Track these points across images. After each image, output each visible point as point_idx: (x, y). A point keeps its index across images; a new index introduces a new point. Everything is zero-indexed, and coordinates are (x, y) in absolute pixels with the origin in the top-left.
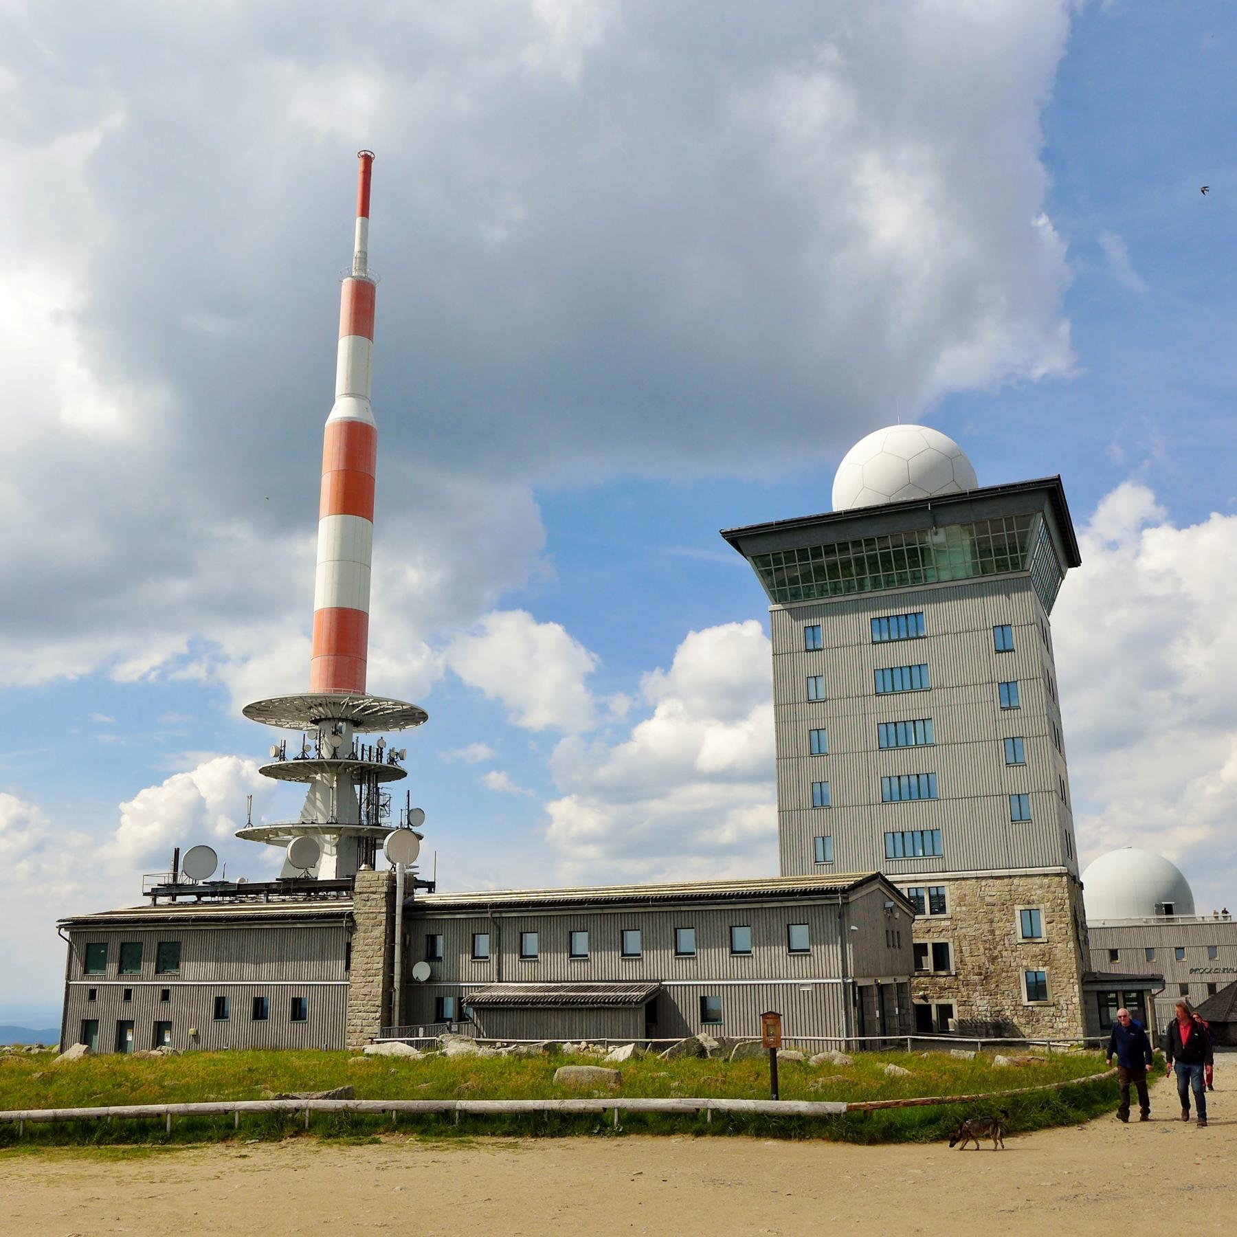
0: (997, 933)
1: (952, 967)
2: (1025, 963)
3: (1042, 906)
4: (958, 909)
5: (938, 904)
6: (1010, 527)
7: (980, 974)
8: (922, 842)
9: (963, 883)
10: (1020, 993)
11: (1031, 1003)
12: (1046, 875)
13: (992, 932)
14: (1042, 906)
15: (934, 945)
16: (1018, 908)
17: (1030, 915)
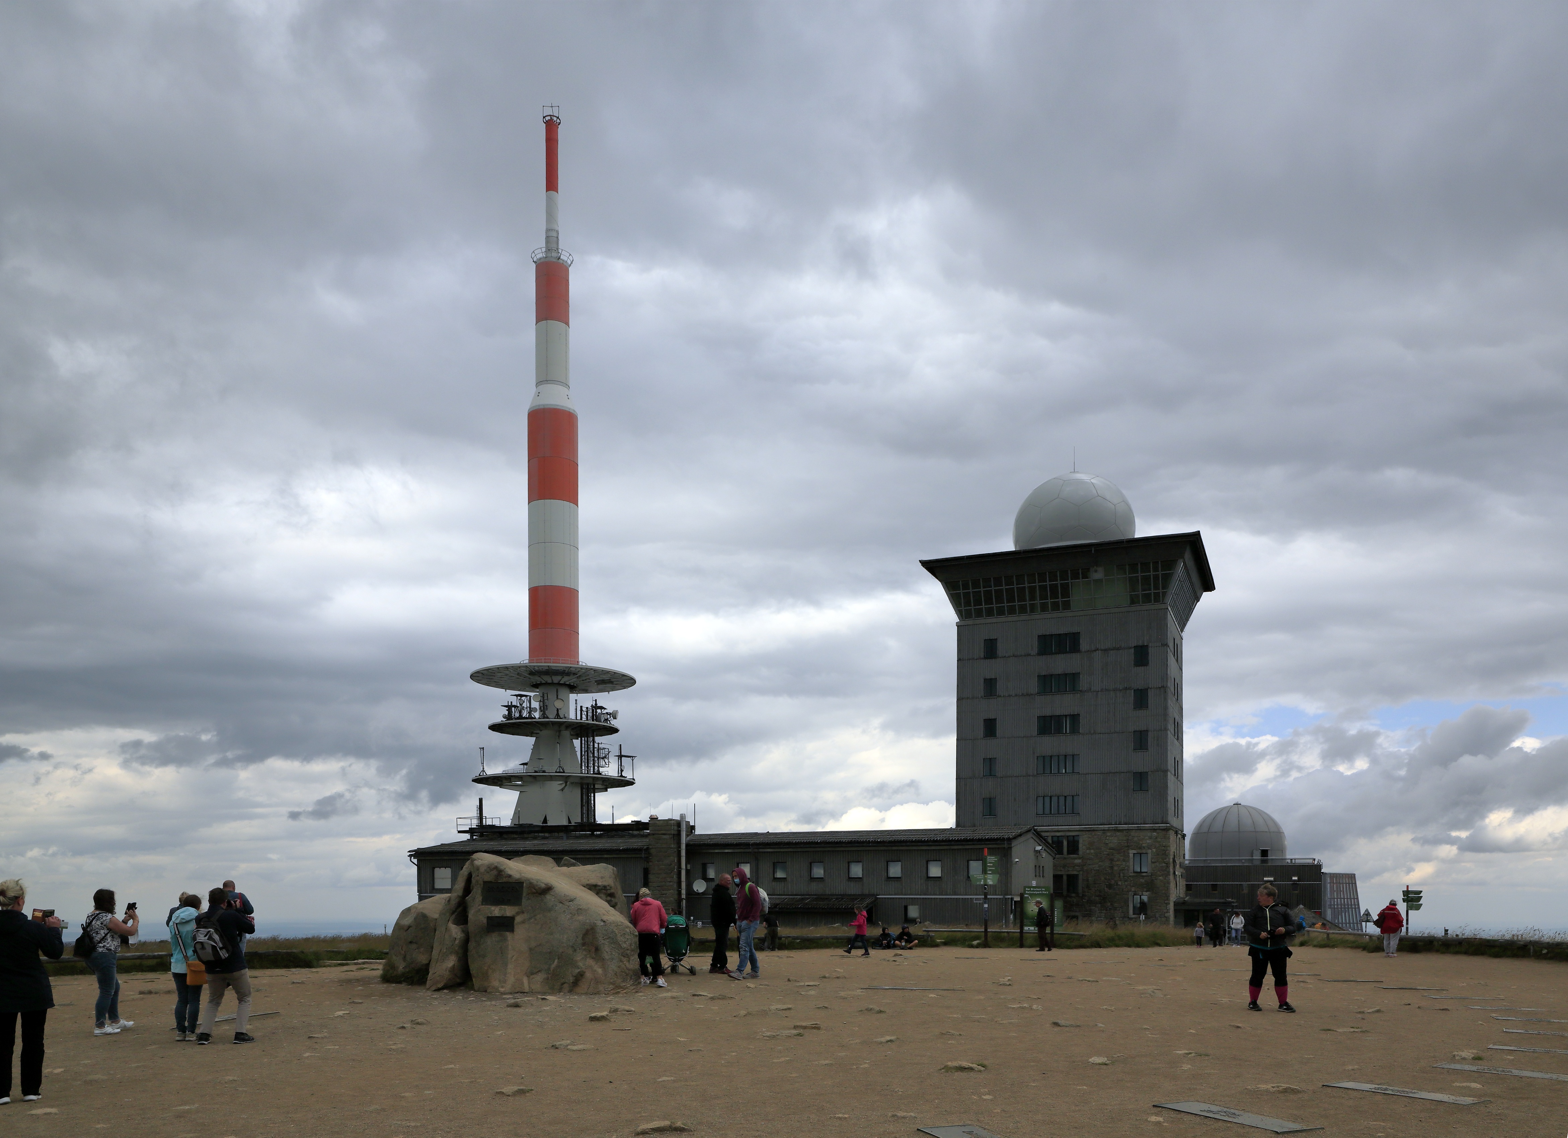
0: (1116, 868)
4: (1088, 851)
5: (1073, 847)
6: (1156, 569)
12: (1154, 830)
13: (1112, 868)
14: (1149, 851)
15: (1069, 876)
16: (1132, 852)
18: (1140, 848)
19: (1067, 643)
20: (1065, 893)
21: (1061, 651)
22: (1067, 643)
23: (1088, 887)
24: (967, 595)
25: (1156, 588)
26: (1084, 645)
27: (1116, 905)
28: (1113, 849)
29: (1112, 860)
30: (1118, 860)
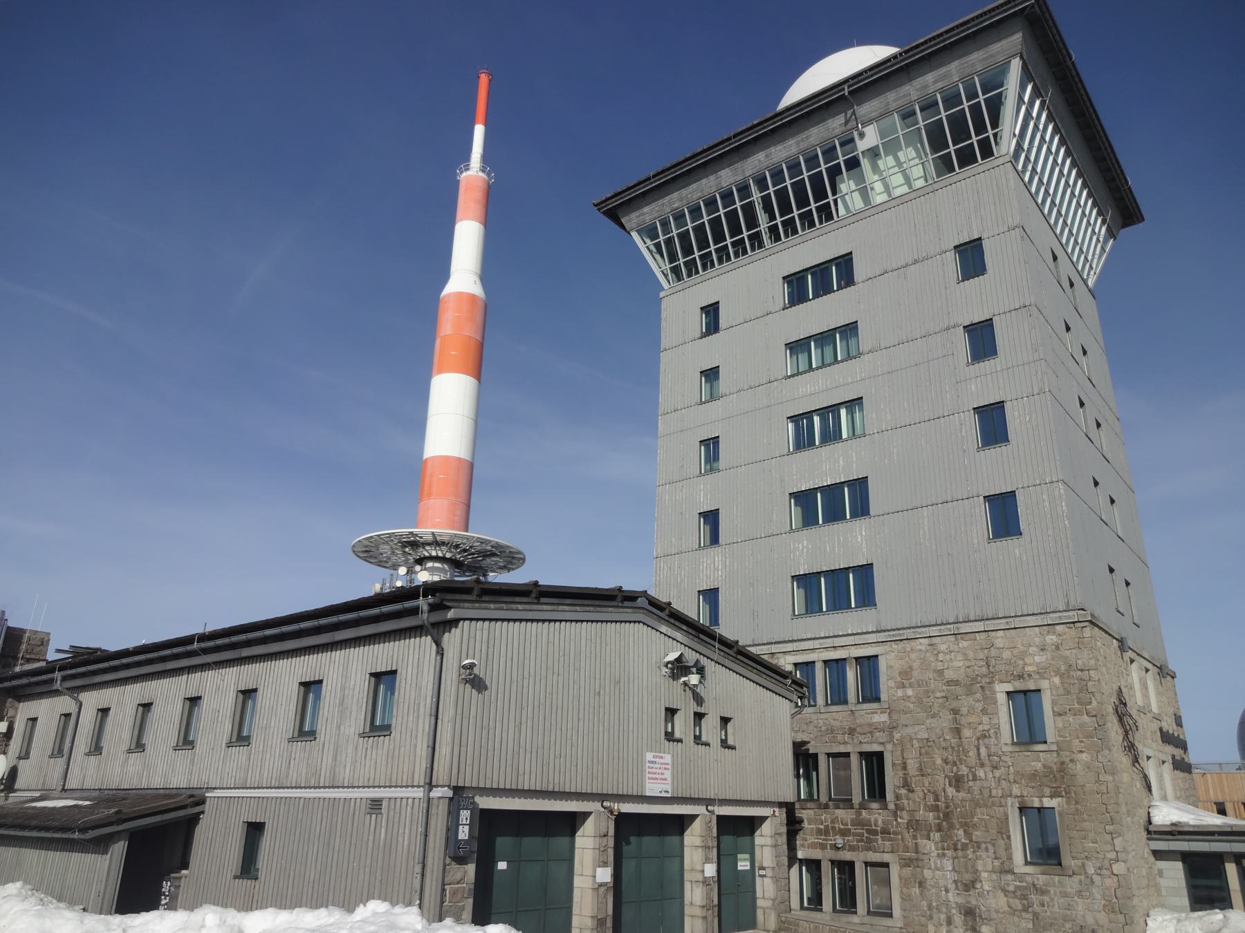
0: (966, 733)
1: (890, 796)
2: (1016, 790)
3: (1044, 685)
4: (900, 693)
7: (936, 808)
8: (844, 587)
9: (908, 646)
10: (1008, 848)
11: (1029, 869)
13: (957, 732)
17: (1025, 700)
18: (1020, 677)
20: (857, 799)
21: (824, 288)
23: (906, 784)
25: (981, 128)
26: (859, 271)
27: (977, 835)
28: (956, 683)
29: (955, 712)
30: (971, 711)
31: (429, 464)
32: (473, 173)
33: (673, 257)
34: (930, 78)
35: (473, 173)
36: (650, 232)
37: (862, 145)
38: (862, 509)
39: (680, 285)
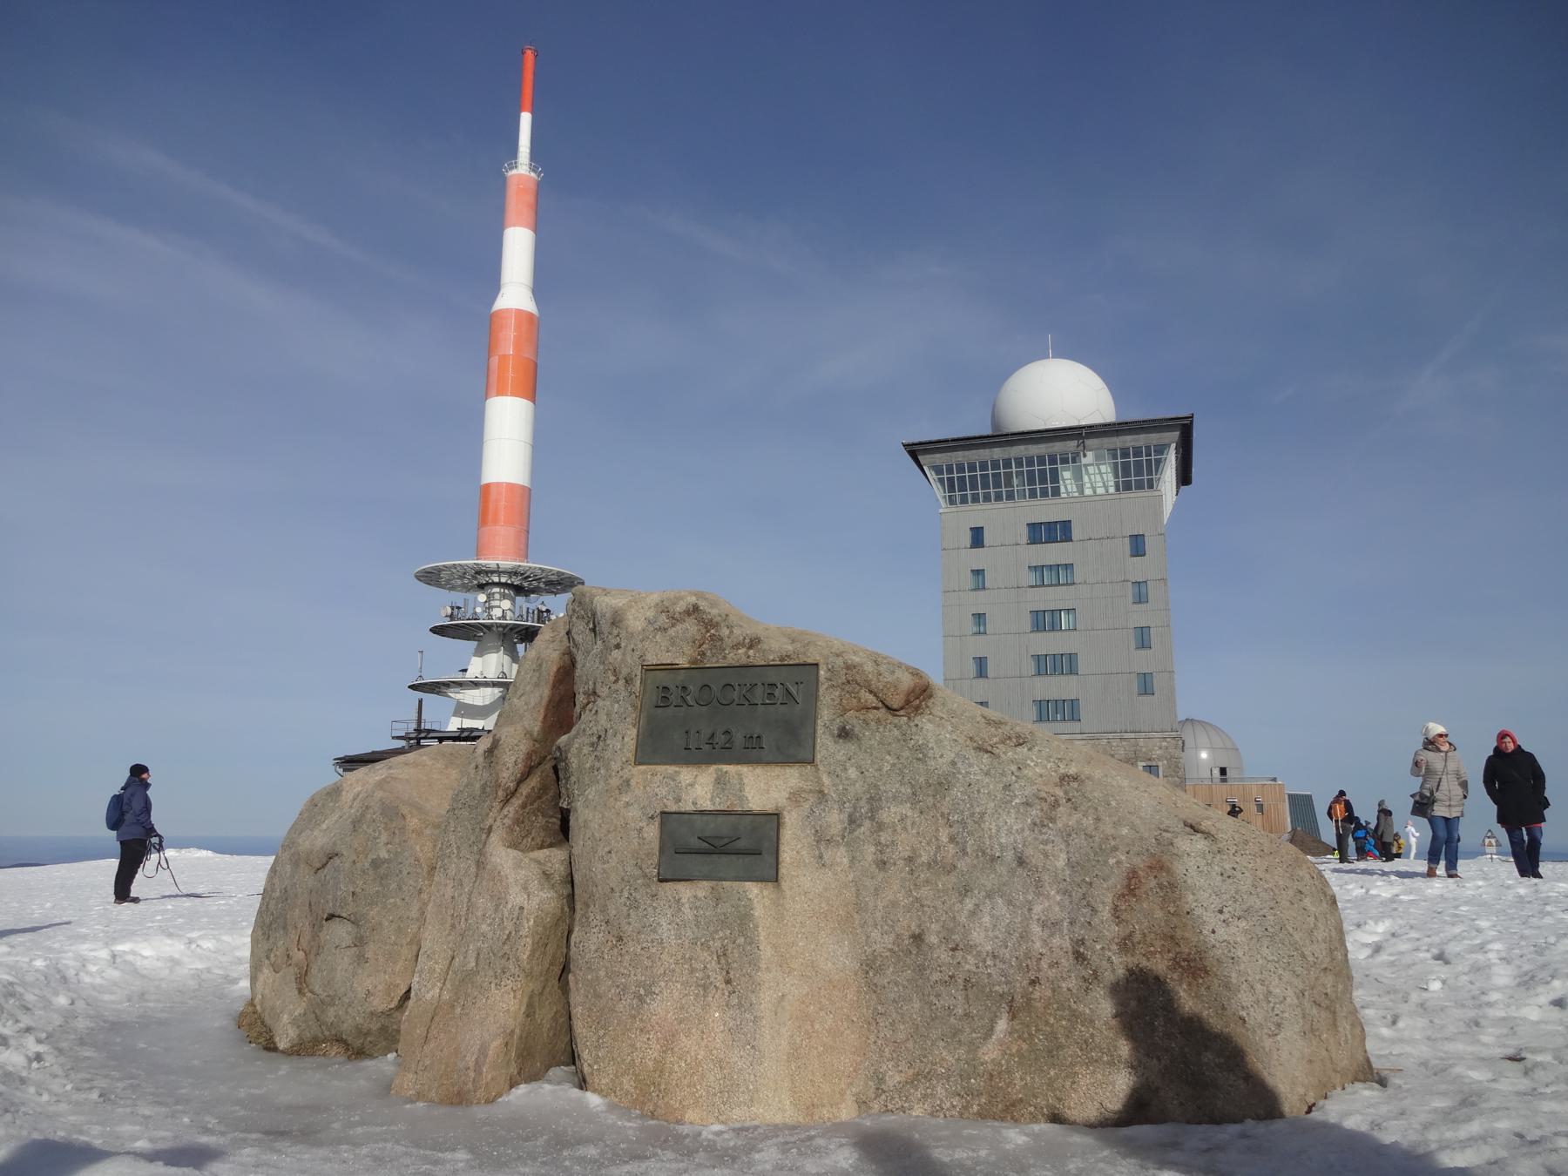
19: (1058, 532)
22: (1058, 532)
24: (951, 480)
26: (1076, 534)
31: (493, 491)
32: (523, 167)
33: (952, 488)
34: (1129, 438)
35: (523, 167)
36: (938, 470)
37: (1084, 461)
38: (1073, 671)
39: (953, 509)
